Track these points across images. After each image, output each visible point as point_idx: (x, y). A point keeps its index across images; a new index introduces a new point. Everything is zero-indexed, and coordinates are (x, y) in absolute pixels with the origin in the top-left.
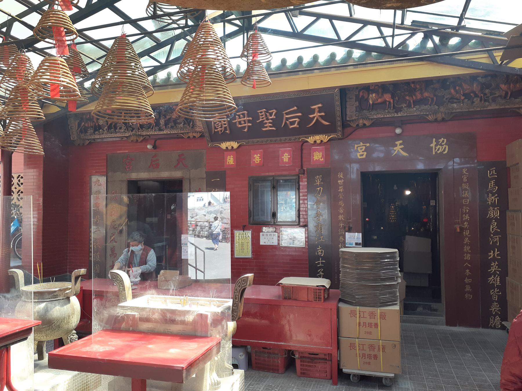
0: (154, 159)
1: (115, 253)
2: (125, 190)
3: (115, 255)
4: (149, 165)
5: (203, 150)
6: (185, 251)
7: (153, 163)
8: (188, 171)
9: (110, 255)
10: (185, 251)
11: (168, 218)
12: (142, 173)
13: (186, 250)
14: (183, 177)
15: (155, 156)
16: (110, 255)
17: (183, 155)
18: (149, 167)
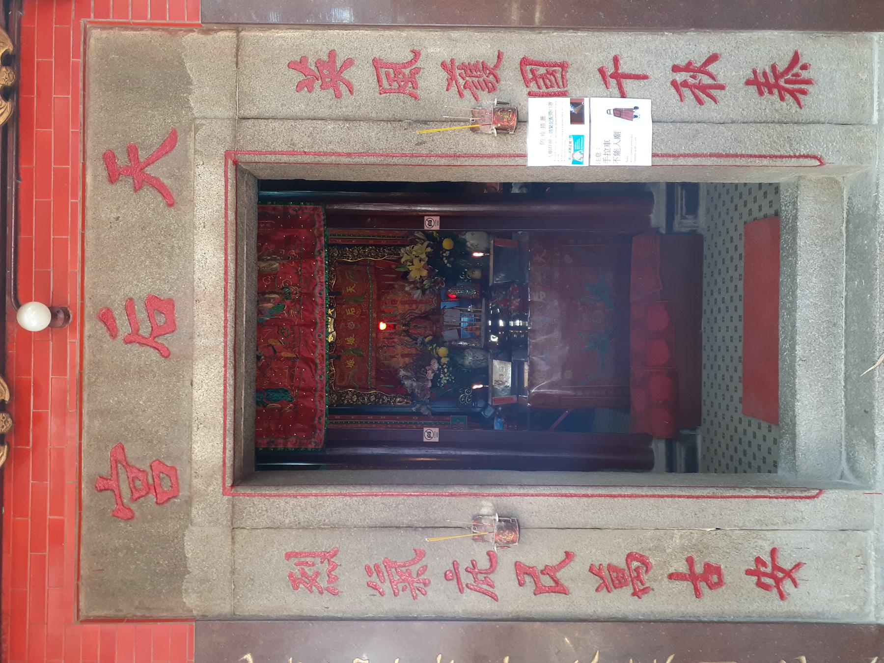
0: (124, 327)
1: (622, 565)
2: (281, 502)
3: (635, 564)
4: (154, 355)
5: (92, 42)
6: (613, 147)
7: (145, 330)
8: (197, 129)
9: (634, 594)
10: (613, 147)
11: (436, 439)
12: (196, 394)
13: (607, 143)
14: (227, 154)
15: (106, 318)
16: (634, 594)
17: (109, 159)
18: (165, 354)
